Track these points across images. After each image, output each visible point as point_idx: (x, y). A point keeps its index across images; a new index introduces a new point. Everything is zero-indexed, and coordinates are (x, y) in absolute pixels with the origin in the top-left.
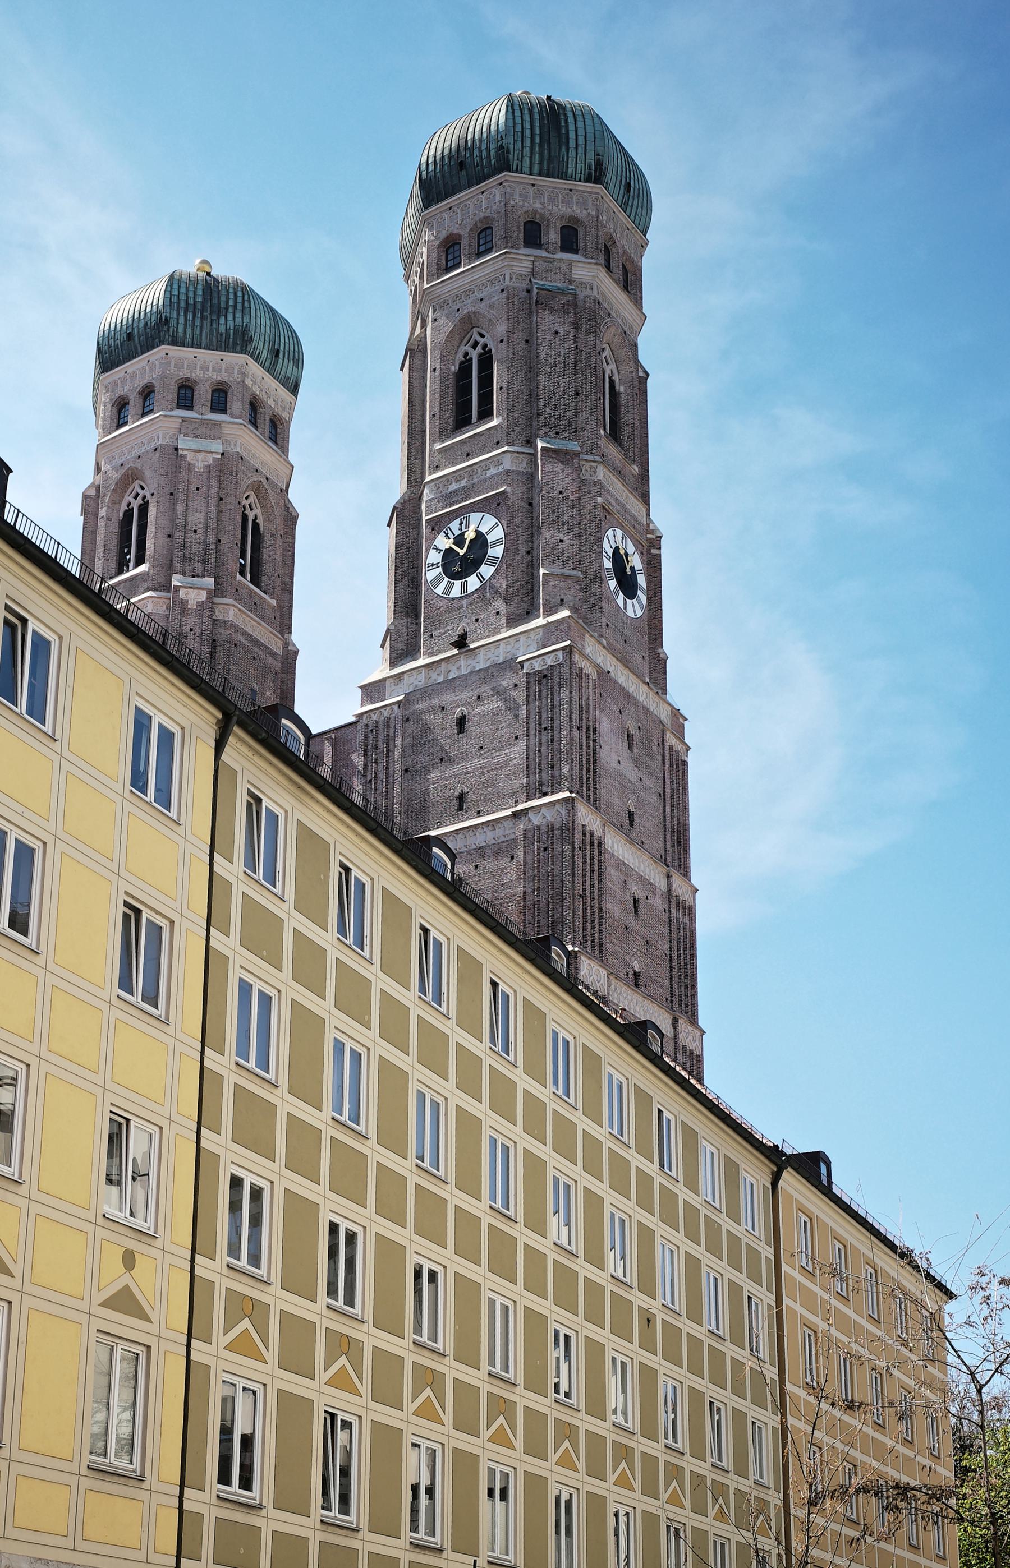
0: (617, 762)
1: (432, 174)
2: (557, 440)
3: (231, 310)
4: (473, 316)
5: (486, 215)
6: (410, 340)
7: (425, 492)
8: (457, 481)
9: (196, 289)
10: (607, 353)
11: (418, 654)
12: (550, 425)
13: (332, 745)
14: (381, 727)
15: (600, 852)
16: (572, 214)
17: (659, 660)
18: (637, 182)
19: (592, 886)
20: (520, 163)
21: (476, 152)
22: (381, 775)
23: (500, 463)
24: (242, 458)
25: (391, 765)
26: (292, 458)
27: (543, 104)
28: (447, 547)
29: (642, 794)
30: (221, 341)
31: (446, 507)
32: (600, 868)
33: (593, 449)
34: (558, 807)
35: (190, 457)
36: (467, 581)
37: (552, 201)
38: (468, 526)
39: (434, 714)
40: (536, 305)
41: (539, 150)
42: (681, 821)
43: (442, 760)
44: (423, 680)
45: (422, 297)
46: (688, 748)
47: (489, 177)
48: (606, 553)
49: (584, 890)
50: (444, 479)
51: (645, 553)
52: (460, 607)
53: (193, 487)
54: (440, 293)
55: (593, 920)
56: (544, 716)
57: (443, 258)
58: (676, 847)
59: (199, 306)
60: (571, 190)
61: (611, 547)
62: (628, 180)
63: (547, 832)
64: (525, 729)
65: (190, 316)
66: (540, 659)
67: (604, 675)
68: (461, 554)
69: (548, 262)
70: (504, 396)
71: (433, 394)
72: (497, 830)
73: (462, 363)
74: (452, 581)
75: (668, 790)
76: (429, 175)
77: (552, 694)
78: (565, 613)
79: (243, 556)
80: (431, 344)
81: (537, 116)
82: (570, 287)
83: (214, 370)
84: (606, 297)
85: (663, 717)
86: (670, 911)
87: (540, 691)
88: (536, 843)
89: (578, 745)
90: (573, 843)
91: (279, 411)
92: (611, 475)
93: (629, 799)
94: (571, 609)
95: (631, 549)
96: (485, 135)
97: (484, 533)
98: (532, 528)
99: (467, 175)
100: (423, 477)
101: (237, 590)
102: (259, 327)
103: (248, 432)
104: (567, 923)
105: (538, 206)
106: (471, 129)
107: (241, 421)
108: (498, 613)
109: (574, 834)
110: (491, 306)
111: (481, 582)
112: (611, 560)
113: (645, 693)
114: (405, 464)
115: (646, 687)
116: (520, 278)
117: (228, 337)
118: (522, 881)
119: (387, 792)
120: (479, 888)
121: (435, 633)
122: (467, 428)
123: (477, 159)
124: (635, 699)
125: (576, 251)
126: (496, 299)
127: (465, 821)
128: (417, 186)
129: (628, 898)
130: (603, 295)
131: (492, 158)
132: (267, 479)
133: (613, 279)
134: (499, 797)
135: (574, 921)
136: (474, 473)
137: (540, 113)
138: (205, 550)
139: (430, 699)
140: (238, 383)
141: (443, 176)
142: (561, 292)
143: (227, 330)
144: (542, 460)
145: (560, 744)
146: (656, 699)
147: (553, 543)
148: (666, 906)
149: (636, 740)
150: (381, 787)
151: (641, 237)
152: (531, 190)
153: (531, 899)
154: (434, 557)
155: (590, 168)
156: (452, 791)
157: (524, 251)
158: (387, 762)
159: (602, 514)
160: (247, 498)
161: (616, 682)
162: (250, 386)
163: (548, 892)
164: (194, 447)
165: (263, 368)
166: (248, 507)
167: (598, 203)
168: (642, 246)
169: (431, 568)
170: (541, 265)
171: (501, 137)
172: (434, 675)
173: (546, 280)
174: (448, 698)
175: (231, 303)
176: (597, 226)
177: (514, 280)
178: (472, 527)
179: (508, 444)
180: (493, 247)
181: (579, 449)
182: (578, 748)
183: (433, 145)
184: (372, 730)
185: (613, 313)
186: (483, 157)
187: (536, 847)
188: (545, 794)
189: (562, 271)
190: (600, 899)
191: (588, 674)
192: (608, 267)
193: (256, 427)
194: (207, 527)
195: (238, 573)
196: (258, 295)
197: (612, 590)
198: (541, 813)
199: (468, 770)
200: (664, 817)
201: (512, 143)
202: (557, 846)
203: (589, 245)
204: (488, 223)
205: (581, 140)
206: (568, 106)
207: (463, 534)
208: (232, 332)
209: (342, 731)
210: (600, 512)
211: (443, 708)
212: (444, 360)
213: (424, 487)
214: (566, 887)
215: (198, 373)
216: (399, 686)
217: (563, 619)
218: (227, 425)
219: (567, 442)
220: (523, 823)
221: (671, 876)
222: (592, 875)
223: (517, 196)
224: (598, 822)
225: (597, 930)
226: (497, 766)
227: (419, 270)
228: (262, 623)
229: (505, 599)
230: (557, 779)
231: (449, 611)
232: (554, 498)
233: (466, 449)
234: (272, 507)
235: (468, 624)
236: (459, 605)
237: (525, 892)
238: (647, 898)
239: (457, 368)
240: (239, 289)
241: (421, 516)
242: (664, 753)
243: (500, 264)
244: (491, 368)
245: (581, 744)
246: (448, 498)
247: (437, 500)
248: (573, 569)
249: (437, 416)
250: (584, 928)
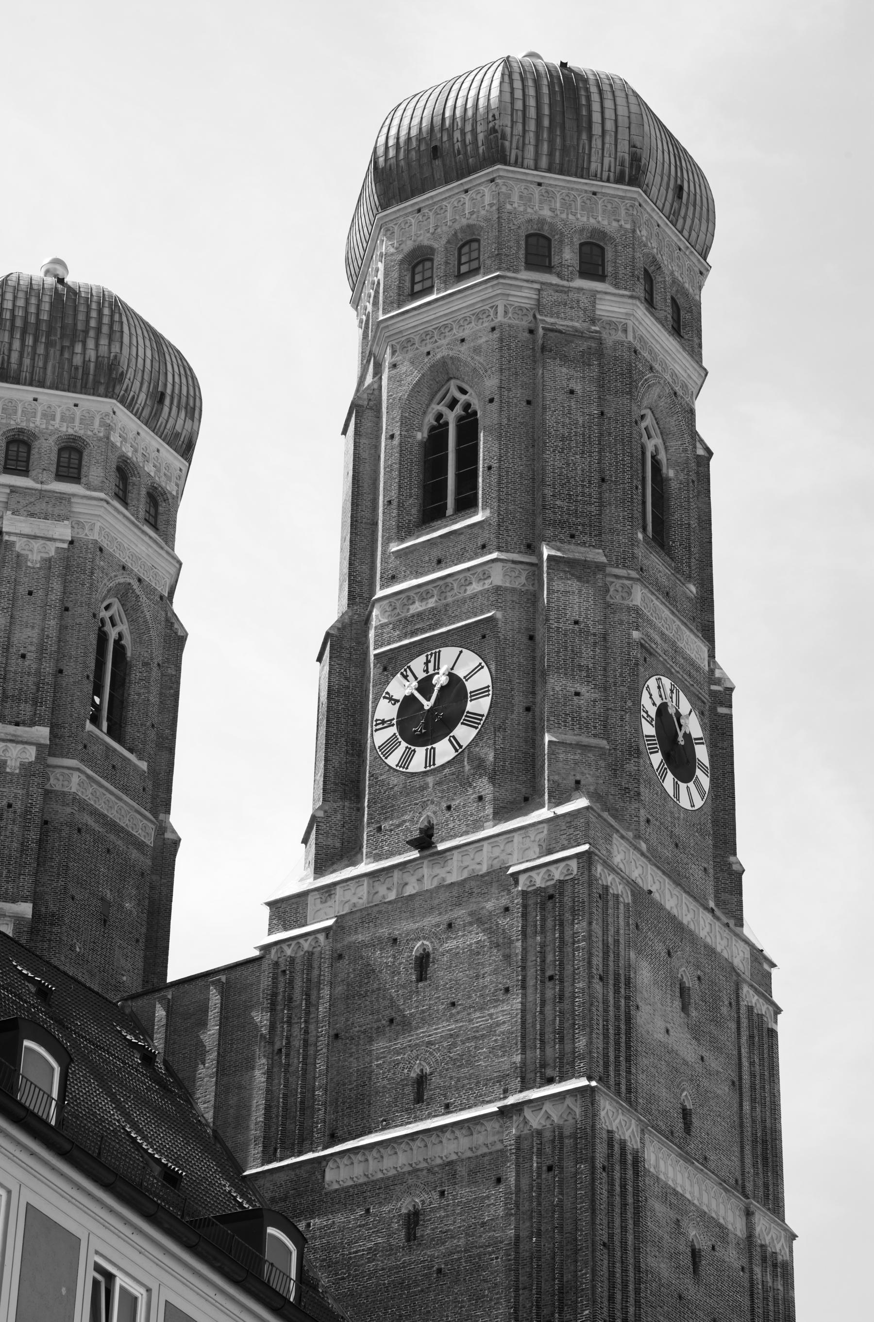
0: (663, 1031)
1: (393, 161)
2: (572, 547)
3: (92, 333)
4: (449, 362)
5: (471, 222)
6: (358, 390)
7: (374, 614)
8: (422, 599)
9: (40, 301)
10: (649, 421)
11: (359, 856)
12: (562, 524)
13: (222, 993)
14: (298, 967)
15: (636, 1173)
16: (596, 226)
17: (730, 874)
18: (692, 184)
19: (624, 1229)
20: (520, 153)
21: (457, 135)
22: (297, 1043)
23: (486, 576)
24: (101, 550)
25: (312, 1027)
26: (180, 550)
27: (555, 74)
28: (407, 692)
29: (705, 1083)
30: (76, 378)
31: (405, 636)
32: (637, 1201)
33: (626, 560)
34: (569, 1101)
35: (20, 545)
36: (434, 749)
37: (567, 206)
38: (437, 667)
39: (381, 949)
40: (542, 352)
41: (549, 137)
42: (768, 1124)
43: (391, 1021)
44: (365, 898)
45: (376, 332)
46: (778, 1010)
47: (475, 170)
49: (611, 1236)
50: (403, 596)
51: (706, 713)
52: (424, 787)
53: (22, 590)
54: (402, 328)
55: (625, 1285)
56: (550, 958)
57: (408, 278)
58: (760, 1166)
59: (44, 327)
60: (594, 193)
61: (654, 704)
62: (679, 182)
63: (553, 1141)
64: (520, 978)
65: (30, 341)
66: (544, 870)
67: (642, 896)
68: (426, 708)
69: (561, 292)
70: (494, 479)
71: (389, 469)
72: (475, 1136)
73: (432, 429)
74: (413, 748)
75: (746, 1077)
76: (389, 163)
77: (562, 925)
78: (581, 803)
79: (98, 690)
80: (388, 400)
81: (545, 90)
82: (593, 328)
83: (63, 419)
84: (646, 343)
85: (737, 962)
86: (751, 1271)
87: (544, 920)
88: (535, 1158)
89: (601, 1005)
90: (593, 1159)
91: (162, 481)
92: (653, 598)
93: (683, 1090)
94: (590, 796)
95: (685, 706)
96: (470, 113)
97: (462, 678)
98: (534, 673)
99: (444, 165)
100: (372, 592)
101: (85, 747)
102: (134, 360)
103: (113, 512)
104: (583, 1290)
105: (546, 213)
106: (450, 103)
107: (102, 495)
108: (480, 798)
109: (594, 1145)
110: (477, 350)
111: (456, 750)
112: (654, 723)
113: (707, 925)
114: (346, 571)
115: (709, 916)
116: (520, 312)
117: (86, 373)
118: (513, 1218)
119: (305, 1070)
120: (446, 1228)
121: (385, 825)
122: (439, 522)
123: (457, 146)
124: (691, 933)
125: (602, 278)
126: (484, 339)
127: (426, 1119)
128: (371, 176)
129: (682, 1248)
131: (480, 144)
132: (140, 580)
133: (657, 319)
134: (478, 1082)
135: (594, 1287)
136: (448, 589)
137: (551, 85)
138: (37, 685)
139: (376, 926)
140: (100, 439)
141: (409, 164)
142: (578, 334)
143: (85, 363)
144: (548, 574)
145: (573, 1002)
146: (726, 933)
147: (565, 697)
148: (744, 1262)
149: (695, 997)
150: (296, 1061)
151: (699, 260)
152: (537, 190)
153: (527, 1247)
154: (386, 710)
155: (622, 164)
156: (406, 1071)
157: (525, 275)
158: (306, 1022)
159: (639, 656)
160: (107, 608)
161: (661, 908)
162: (118, 444)
163: (553, 1238)
164: (27, 530)
165: (139, 419)
166: (108, 621)
167: (635, 213)
168: (701, 273)
169: (380, 726)
171: (494, 116)
172: (382, 890)
173: (558, 318)
174: (404, 927)
175: (93, 323)
176: (633, 244)
177: (510, 315)
178: (444, 668)
179: (499, 549)
180: (479, 268)
181: (603, 559)
182: (601, 1009)
183: (396, 122)
184: (284, 971)
186: (467, 142)
187: (535, 1165)
188: (550, 1081)
189: (582, 305)
190: (637, 1250)
191: (618, 895)
192: (650, 302)
193: (124, 501)
194: (42, 649)
195: (88, 721)
196: (135, 313)
197: (656, 767)
198: (543, 1111)
199: (432, 1039)
200: (741, 1118)
201: (509, 125)
202: (568, 1164)
203: (621, 271)
204: (474, 234)
205: (610, 125)
206: (591, 77)
207: (430, 677)
208: (92, 366)
209: (238, 972)
210: (637, 653)
211: (395, 940)
212: (407, 424)
213: (373, 606)
214: (581, 1230)
215: (38, 423)
216: (329, 903)
217: (579, 811)
218: (80, 501)
219: (588, 549)
220: (515, 1125)
221: (753, 1213)
222: (623, 1212)
223: (515, 198)
224: (633, 1126)
225: (631, 1300)
226: (477, 1034)
227: (372, 292)
228: (124, 797)
229: (492, 780)
230: (568, 1058)
231: (407, 791)
232: (566, 630)
233: (436, 553)
234: (146, 622)
235: (435, 813)
236: (422, 783)
237: (517, 1237)
238: (713, 1248)
239: (426, 435)
240: (106, 304)
241: (368, 647)
242: (739, 1017)
243: (490, 293)
244: (476, 438)
245: (605, 1002)
246: (408, 625)
247: (391, 626)
248: (595, 736)
249: (395, 503)
250: (611, 1298)
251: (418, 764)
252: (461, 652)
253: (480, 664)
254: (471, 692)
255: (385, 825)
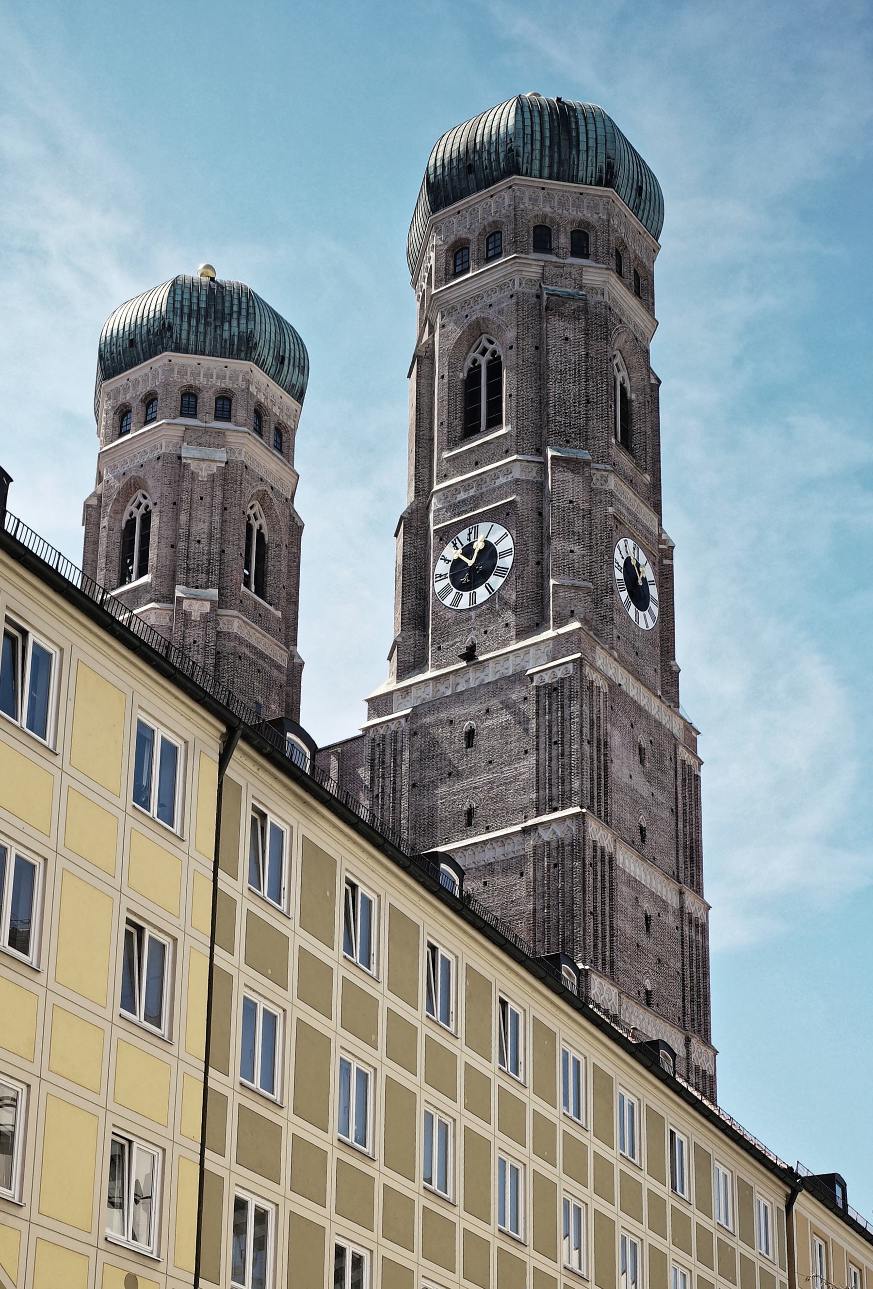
1: (440, 177)
2: (568, 449)
3: (235, 316)
4: (482, 322)
5: (495, 219)
6: (417, 346)
7: (433, 502)
8: (465, 490)
9: (199, 294)
11: (426, 666)
12: (560, 433)
13: (338, 760)
14: (388, 741)
16: (583, 218)
20: (529, 167)
21: (485, 155)
22: (389, 790)
23: (509, 472)
24: (246, 467)
25: (398, 780)
27: (553, 107)
28: (455, 557)
30: (225, 348)
31: (454, 517)
33: (605, 458)
35: (193, 466)
36: (475, 593)
37: (562, 204)
38: (476, 537)
39: (442, 727)
40: (546, 311)
41: (550, 153)
43: (450, 774)
44: (431, 693)
45: (430, 303)
47: (498, 181)
48: (618, 563)
50: (452, 488)
52: (469, 619)
53: (196, 497)
54: (448, 299)
56: (554, 730)
57: (452, 262)
59: (203, 312)
60: (581, 194)
64: (535, 743)
65: (194, 322)
66: (550, 671)
68: (470, 565)
69: (559, 267)
70: (514, 404)
71: (441, 402)
73: (470, 370)
74: (461, 592)
76: (437, 179)
77: (562, 707)
78: (575, 625)
79: (247, 566)
80: (439, 351)
81: (547, 118)
82: (581, 292)
83: (218, 378)
84: (617, 303)
87: (550, 705)
92: (622, 484)
94: (581, 621)
96: (494, 138)
97: (493, 543)
98: (542, 538)
99: (476, 178)
100: (431, 486)
101: (241, 602)
102: (263, 334)
105: (548, 210)
106: (480, 132)
107: (246, 429)
108: (507, 625)
111: (490, 593)
114: (413, 473)
116: (530, 283)
117: (231, 344)
121: (443, 645)
122: (476, 436)
123: (486, 163)
125: (586, 256)
126: (505, 304)
128: (425, 190)
130: (614, 300)
131: (501, 161)
132: (272, 488)
133: (625, 285)
136: (483, 482)
137: (550, 115)
138: (209, 560)
139: (438, 713)
140: (243, 390)
141: (451, 180)
142: (571, 297)
143: (231, 337)
144: (552, 468)
152: (541, 193)
154: (443, 568)
155: (601, 171)
157: (533, 256)
158: (394, 776)
159: (613, 524)
160: (251, 508)
162: (255, 393)
164: (197, 455)
165: (268, 375)
166: (252, 517)
167: (609, 207)
169: (439, 579)
170: (551, 271)
171: (511, 139)
172: (442, 688)
173: (557, 286)
174: (456, 712)
175: (235, 308)
176: (609, 230)
177: (523, 285)
178: (481, 537)
179: (517, 453)
180: (502, 252)
181: (590, 458)
183: (441, 148)
184: (379, 745)
185: (624, 319)
186: (492, 160)
192: (619, 272)
193: (260, 434)
194: (210, 536)
195: (242, 585)
196: (263, 301)
201: (522, 145)
203: (600, 250)
204: (497, 228)
205: (592, 143)
206: (579, 108)
207: (471, 544)
209: (349, 745)
210: (611, 522)
211: (451, 722)
212: (452, 367)
213: (432, 496)
215: (201, 381)
216: (407, 699)
217: (574, 631)
218: (231, 434)
219: (577, 450)
223: (526, 200)
227: (427, 275)
228: (267, 635)
229: (515, 611)
231: (457, 622)
232: (564, 507)
233: (474, 457)
234: (277, 516)
235: (476, 636)
236: (468, 616)
239: (466, 375)
240: (244, 295)
241: (429, 526)
243: (510, 269)
244: (501, 375)
246: (456, 508)
247: (445, 509)
248: (584, 580)
249: (445, 424)
251: (464, 603)
252: (493, 525)
253: (506, 533)
254: (500, 553)
255: (443, 645)
